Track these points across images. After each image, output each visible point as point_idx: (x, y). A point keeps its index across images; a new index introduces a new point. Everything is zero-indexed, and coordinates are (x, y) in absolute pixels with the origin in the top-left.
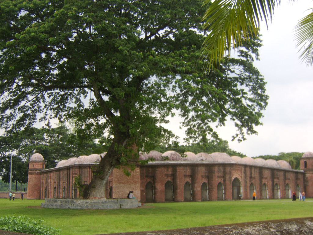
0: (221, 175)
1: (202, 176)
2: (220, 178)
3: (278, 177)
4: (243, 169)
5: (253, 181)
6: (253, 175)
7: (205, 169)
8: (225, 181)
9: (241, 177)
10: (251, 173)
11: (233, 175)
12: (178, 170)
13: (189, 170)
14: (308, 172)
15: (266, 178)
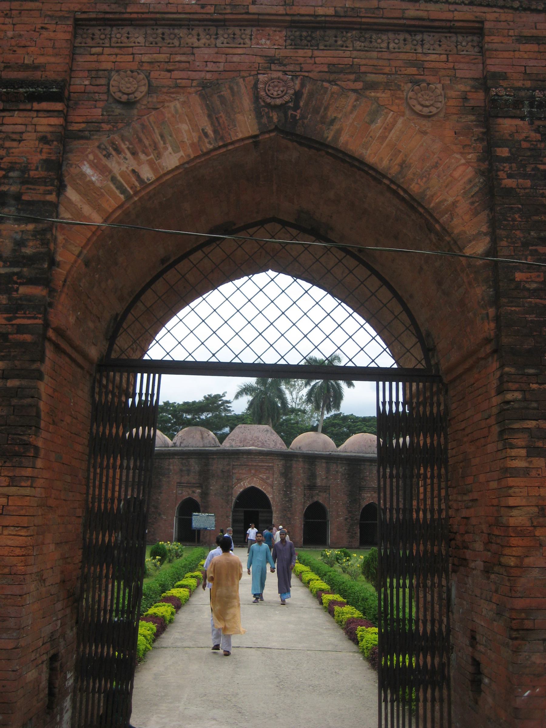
5: (320, 498)
8: (205, 495)
10: (312, 476)
11: (239, 480)
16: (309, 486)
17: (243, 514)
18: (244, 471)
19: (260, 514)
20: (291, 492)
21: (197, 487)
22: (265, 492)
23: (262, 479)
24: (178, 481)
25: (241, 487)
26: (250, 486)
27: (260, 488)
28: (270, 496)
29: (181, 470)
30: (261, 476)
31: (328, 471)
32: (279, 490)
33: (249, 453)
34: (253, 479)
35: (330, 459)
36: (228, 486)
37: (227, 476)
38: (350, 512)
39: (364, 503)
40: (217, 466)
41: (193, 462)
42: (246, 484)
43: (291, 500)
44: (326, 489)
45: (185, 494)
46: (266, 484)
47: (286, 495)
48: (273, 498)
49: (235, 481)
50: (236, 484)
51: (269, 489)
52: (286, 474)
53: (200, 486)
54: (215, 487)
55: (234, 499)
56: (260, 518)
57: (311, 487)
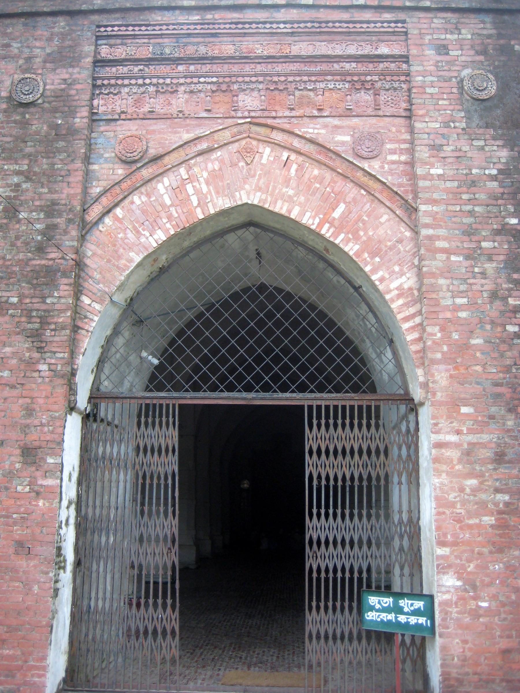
18: (180, 101)
19: (313, 437)
22: (351, 249)
25: (151, 217)
26: (224, 203)
27: (309, 220)
30: (311, 129)
32: (469, 232)
34: (247, 154)
36: (51, 210)
46: (352, 192)
48: (421, 295)
49: (107, 170)
50: (119, 194)
51: (386, 225)
55: (99, 316)
56: (312, 466)
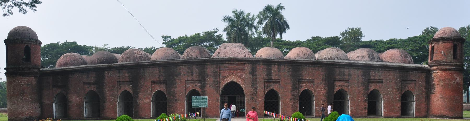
0: (196, 79)
1: (153, 82)
2: (193, 83)
3: (347, 77)
4: (248, 67)
5: (274, 87)
6: (273, 77)
7: (159, 72)
8: (203, 87)
9: (244, 81)
10: (269, 74)
11: (224, 77)
12: (106, 75)
13: (127, 75)
14: (435, 68)
15: (313, 81)
16: (267, 80)
17: (228, 98)
20: (256, 84)
21: (198, 83)
23: (239, 77)
24: (186, 79)
28: (243, 87)
29: (188, 72)
31: (279, 70)
33: (229, 60)
35: (281, 63)
37: (216, 75)
38: (293, 95)
39: (302, 89)
40: (210, 70)
41: (194, 68)
42: (227, 80)
43: (256, 89)
44: (278, 81)
45: (191, 87)
47: (253, 85)
48: (245, 88)
52: (253, 73)
53: (200, 82)
54: (209, 81)
57: (269, 80)
